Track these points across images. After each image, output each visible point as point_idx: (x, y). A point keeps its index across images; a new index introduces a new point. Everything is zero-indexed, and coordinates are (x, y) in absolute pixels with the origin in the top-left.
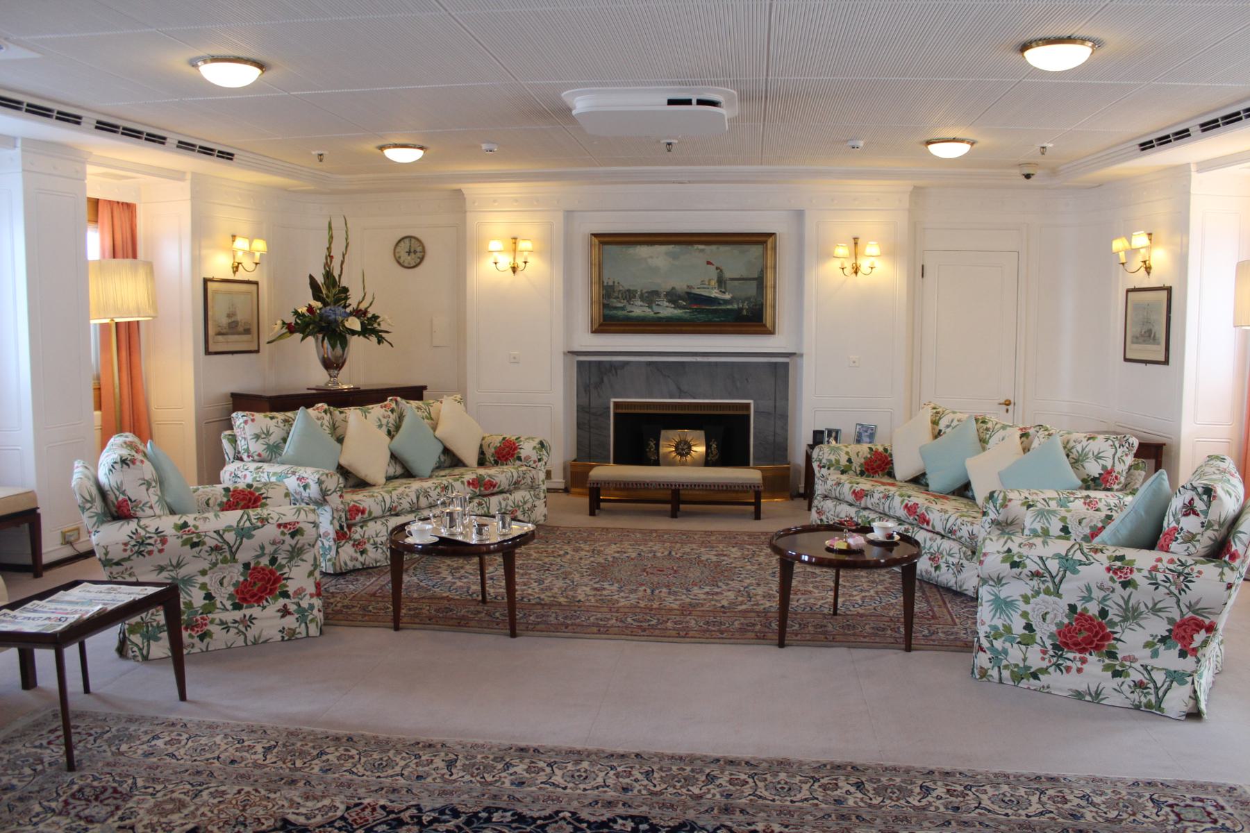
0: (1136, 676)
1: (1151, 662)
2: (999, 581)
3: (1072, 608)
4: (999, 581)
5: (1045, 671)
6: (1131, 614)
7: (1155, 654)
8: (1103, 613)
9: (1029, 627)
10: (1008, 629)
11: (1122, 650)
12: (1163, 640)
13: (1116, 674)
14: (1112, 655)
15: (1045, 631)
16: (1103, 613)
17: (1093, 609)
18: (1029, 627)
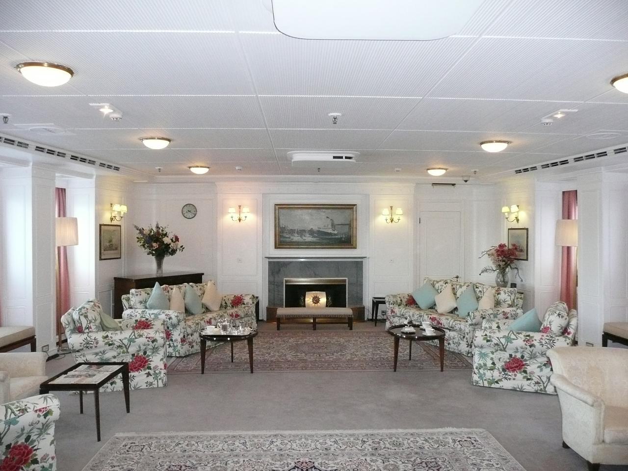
0: (535, 379)
1: (540, 374)
2: (482, 347)
3: (511, 355)
4: (482, 347)
5: (501, 380)
6: (533, 356)
7: (541, 370)
8: (523, 357)
9: (493, 363)
10: (485, 365)
11: (529, 369)
12: (545, 365)
13: (528, 379)
14: (525, 372)
15: (499, 365)
16: (523, 357)
17: (519, 356)
18: (493, 363)
